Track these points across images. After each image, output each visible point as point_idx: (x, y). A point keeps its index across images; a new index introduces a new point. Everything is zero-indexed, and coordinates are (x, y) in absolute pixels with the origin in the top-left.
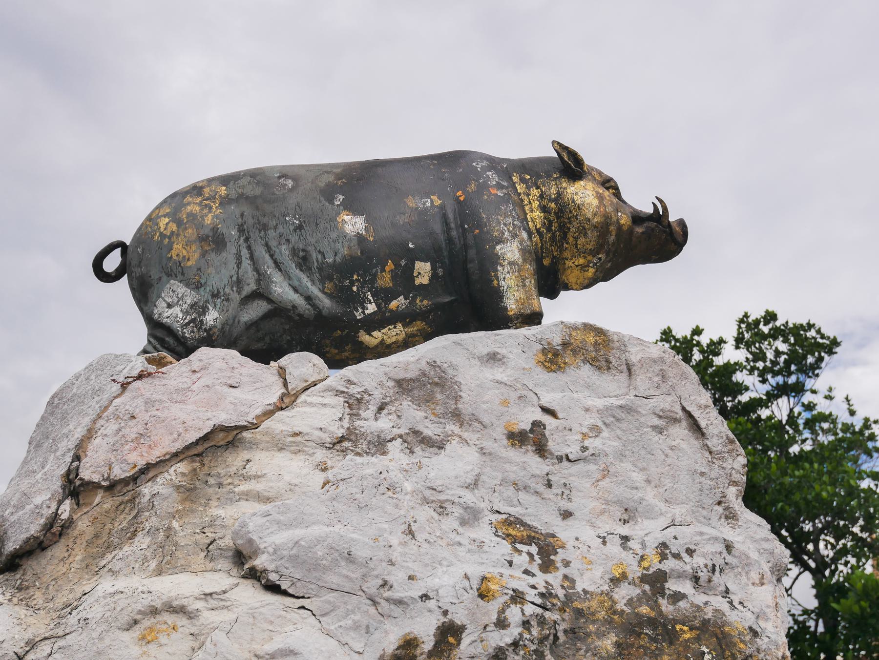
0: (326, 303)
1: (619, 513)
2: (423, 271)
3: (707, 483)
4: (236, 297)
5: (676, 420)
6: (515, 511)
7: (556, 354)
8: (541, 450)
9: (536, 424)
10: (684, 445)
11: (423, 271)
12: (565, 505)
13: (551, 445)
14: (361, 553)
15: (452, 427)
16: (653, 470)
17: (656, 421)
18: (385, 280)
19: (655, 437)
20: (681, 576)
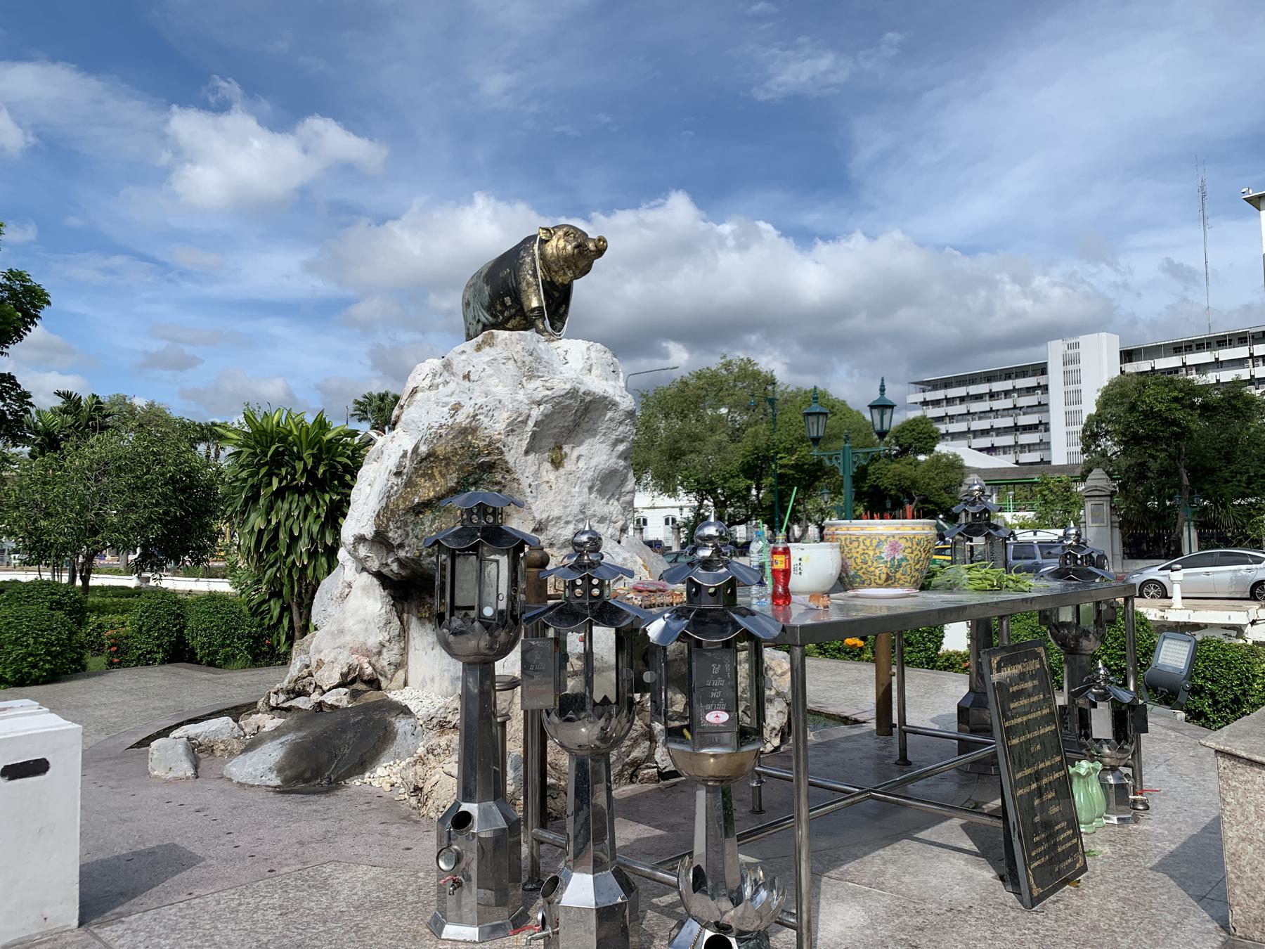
0: (490, 319)
1: (484, 395)
2: (508, 301)
3: (516, 378)
4: (475, 323)
5: (510, 359)
6: (459, 400)
7: (480, 345)
8: (469, 380)
9: (469, 372)
10: (511, 367)
11: (508, 301)
12: (471, 396)
13: (471, 378)
14: (415, 420)
15: (453, 378)
16: (502, 378)
17: (504, 361)
18: (499, 308)
19: (503, 366)
20: (483, 414)
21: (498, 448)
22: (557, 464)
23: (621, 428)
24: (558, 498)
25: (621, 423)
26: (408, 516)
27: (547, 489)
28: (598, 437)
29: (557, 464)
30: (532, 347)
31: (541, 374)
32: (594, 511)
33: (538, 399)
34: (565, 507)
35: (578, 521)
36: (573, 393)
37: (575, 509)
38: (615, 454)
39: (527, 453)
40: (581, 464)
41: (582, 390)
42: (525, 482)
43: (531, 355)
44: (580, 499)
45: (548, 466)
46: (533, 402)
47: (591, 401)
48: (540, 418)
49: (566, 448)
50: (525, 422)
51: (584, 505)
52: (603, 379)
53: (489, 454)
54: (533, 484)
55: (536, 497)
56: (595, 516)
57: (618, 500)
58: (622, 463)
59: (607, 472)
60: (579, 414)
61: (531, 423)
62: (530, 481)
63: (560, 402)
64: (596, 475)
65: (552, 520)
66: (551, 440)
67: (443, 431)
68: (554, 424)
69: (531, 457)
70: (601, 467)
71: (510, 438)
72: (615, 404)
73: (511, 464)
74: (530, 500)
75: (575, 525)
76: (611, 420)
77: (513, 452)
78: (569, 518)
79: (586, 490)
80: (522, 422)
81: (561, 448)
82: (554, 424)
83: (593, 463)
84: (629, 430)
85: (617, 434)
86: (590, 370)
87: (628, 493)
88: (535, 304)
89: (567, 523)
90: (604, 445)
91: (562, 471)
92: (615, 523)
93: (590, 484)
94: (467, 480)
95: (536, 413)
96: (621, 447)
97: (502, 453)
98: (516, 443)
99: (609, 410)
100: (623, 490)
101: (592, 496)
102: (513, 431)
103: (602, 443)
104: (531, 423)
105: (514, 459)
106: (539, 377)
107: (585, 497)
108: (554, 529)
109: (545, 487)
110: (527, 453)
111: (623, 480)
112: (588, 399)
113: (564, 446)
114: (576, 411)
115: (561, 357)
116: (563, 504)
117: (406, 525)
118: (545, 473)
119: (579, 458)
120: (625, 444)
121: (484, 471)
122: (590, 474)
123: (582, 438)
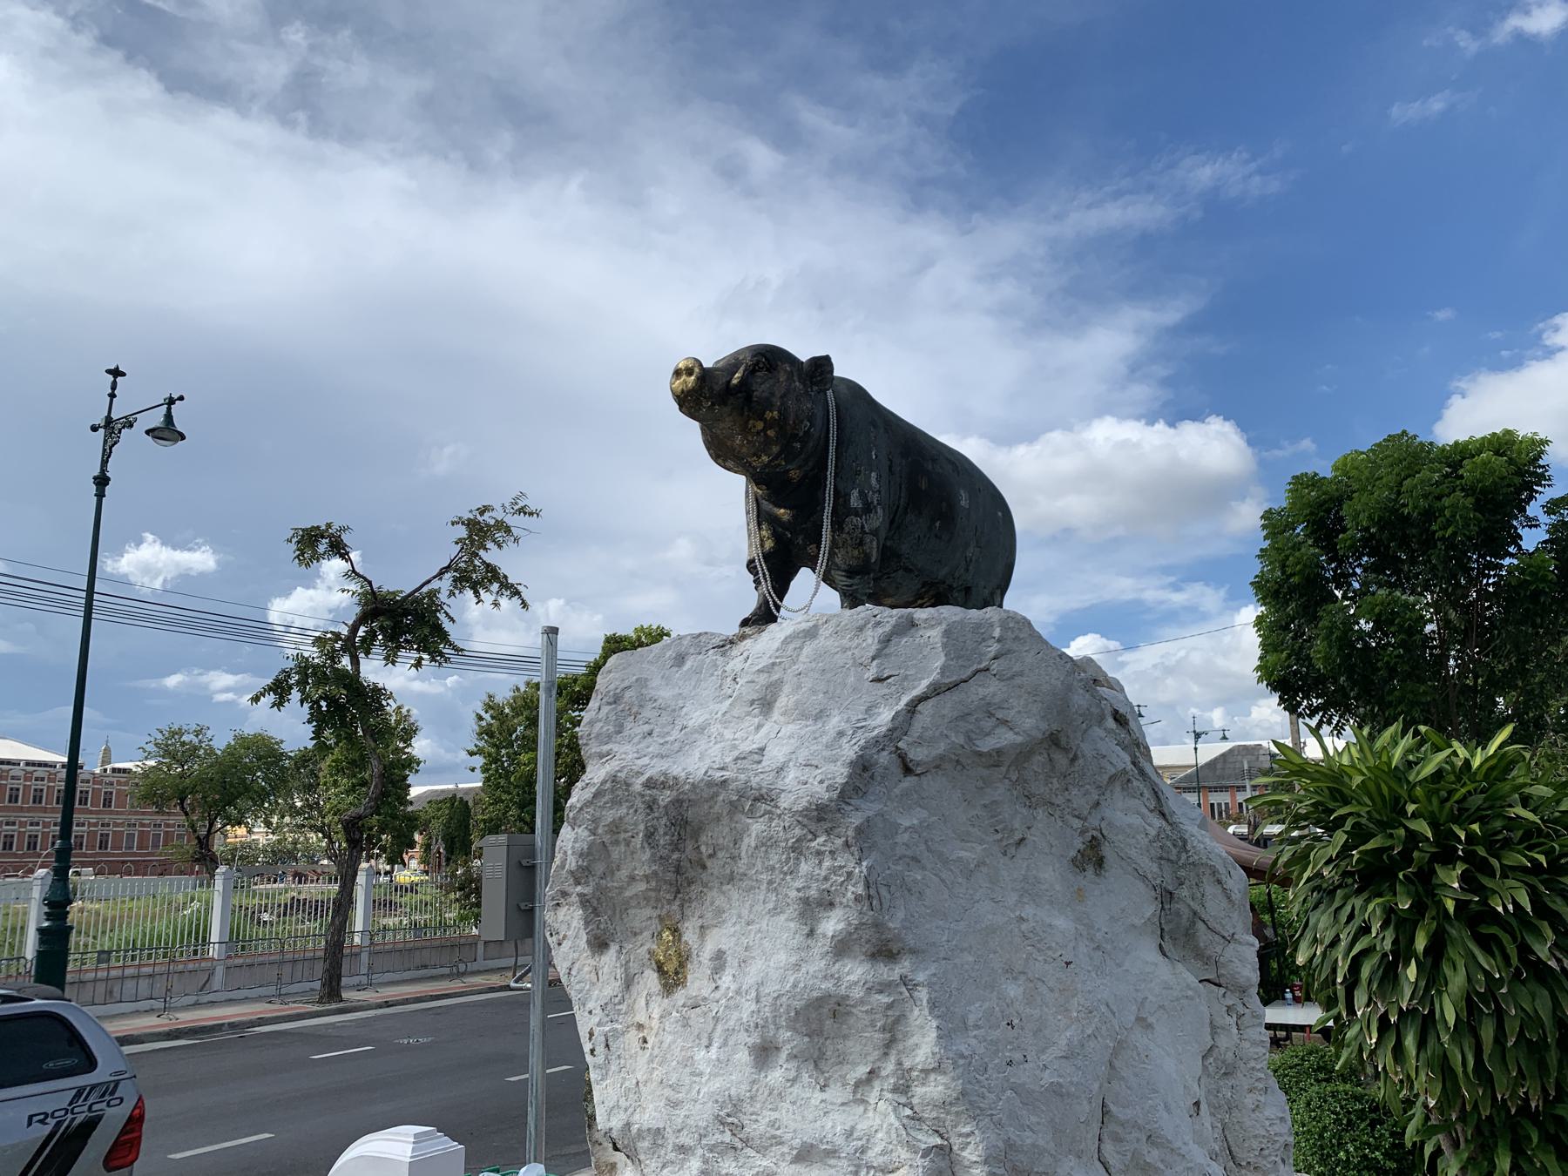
22: (672, 977)
24: (657, 1075)
25: (797, 849)
27: (635, 1045)
29: (672, 977)
32: (772, 1124)
34: (675, 1104)
36: (612, 791)
37: (700, 1113)
38: (821, 946)
44: (717, 1084)
47: (678, 802)
51: (737, 1105)
52: (804, 716)
54: (597, 1031)
59: (798, 1004)
66: (648, 912)
69: (610, 958)
70: (771, 988)
72: (763, 798)
75: (706, 1162)
76: (766, 843)
77: (566, 944)
78: (685, 1139)
79: (743, 1057)
82: (623, 873)
84: (834, 870)
85: (799, 884)
90: (783, 917)
91: (680, 996)
93: (754, 1039)
96: (832, 924)
99: (751, 813)
101: (776, 1075)
105: (567, 964)
107: (738, 1073)
112: (665, 797)
114: (650, 835)
116: (668, 1092)
123: (720, 901)
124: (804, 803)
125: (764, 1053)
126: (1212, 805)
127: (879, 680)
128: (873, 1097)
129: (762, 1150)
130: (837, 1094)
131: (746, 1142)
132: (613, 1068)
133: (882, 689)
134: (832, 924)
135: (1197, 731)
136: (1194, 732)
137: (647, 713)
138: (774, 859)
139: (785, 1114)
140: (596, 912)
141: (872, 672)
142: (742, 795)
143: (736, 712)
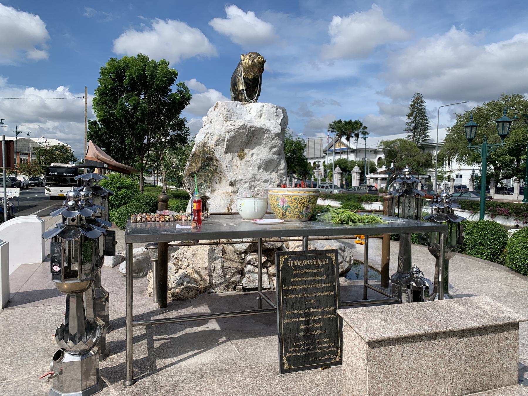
21: (212, 151)
22: (241, 157)
23: (273, 141)
25: (273, 139)
26: (190, 178)
28: (262, 146)
29: (241, 157)
30: (230, 108)
31: (231, 119)
33: (228, 130)
34: (245, 176)
35: (252, 181)
36: (244, 127)
37: (249, 176)
39: (226, 153)
40: (254, 157)
41: (249, 126)
42: (224, 166)
43: (229, 111)
44: (252, 172)
45: (237, 158)
46: (226, 132)
47: (254, 130)
48: (229, 138)
49: (246, 151)
50: (224, 140)
51: (255, 175)
52: (268, 120)
53: (210, 154)
55: (230, 171)
56: (261, 179)
57: (277, 172)
58: (276, 156)
60: (249, 136)
61: (226, 140)
62: (227, 165)
63: (238, 131)
64: (261, 162)
65: (237, 181)
67: (200, 144)
68: (237, 141)
69: (229, 155)
70: (263, 159)
71: (217, 147)
72: (268, 131)
73: (218, 158)
74: (226, 173)
76: (268, 138)
77: (219, 153)
78: (246, 180)
79: (256, 168)
80: (222, 140)
81: (243, 151)
82: (237, 141)
83: (260, 157)
84: (278, 142)
86: (260, 117)
87: (281, 170)
88: (241, 88)
89: (246, 182)
91: (244, 160)
92: (274, 182)
94: (204, 164)
95: (228, 136)
96: (274, 150)
97: (214, 153)
98: (220, 149)
99: (266, 133)
100: (279, 168)
101: (261, 171)
102: (218, 144)
103: (264, 148)
104: (226, 140)
105: (219, 156)
106: (230, 121)
107: (256, 171)
108: (239, 185)
109: (235, 167)
110: (226, 153)
111: (278, 164)
112: (253, 129)
113: (245, 150)
114: (247, 135)
115: (248, 111)
117: (190, 181)
118: (235, 161)
119: (252, 155)
120: (276, 148)
121: (210, 161)
122: (258, 162)
124: (277, 132)
125: (259, 168)
126: (21, 159)
127: (276, 116)
128: (272, 173)
129: (258, 181)
130: (268, 173)
131: (256, 180)
132: (231, 171)
133: (276, 117)
134: (274, 150)
135: (18, 131)
136: (16, 131)
137: (235, 114)
138: (268, 140)
139: (262, 176)
140: (228, 147)
141: (275, 114)
142: (266, 130)
143: (256, 117)
